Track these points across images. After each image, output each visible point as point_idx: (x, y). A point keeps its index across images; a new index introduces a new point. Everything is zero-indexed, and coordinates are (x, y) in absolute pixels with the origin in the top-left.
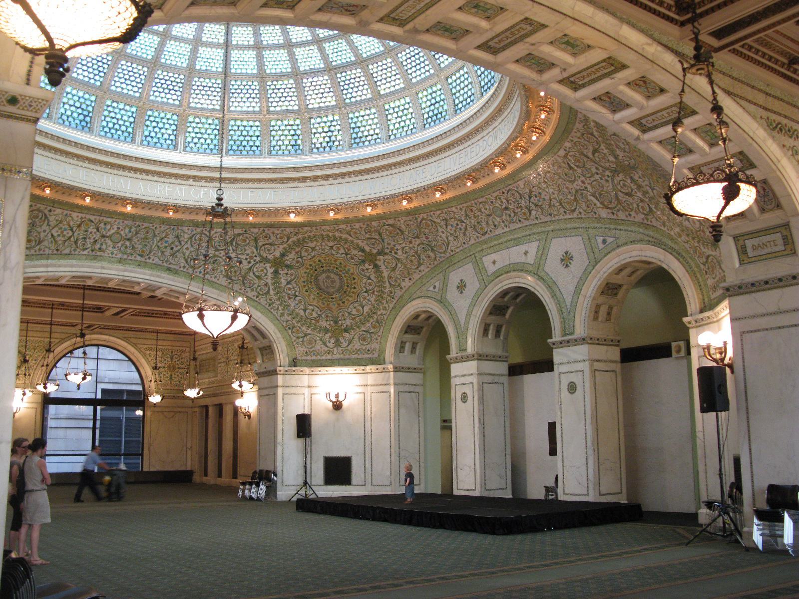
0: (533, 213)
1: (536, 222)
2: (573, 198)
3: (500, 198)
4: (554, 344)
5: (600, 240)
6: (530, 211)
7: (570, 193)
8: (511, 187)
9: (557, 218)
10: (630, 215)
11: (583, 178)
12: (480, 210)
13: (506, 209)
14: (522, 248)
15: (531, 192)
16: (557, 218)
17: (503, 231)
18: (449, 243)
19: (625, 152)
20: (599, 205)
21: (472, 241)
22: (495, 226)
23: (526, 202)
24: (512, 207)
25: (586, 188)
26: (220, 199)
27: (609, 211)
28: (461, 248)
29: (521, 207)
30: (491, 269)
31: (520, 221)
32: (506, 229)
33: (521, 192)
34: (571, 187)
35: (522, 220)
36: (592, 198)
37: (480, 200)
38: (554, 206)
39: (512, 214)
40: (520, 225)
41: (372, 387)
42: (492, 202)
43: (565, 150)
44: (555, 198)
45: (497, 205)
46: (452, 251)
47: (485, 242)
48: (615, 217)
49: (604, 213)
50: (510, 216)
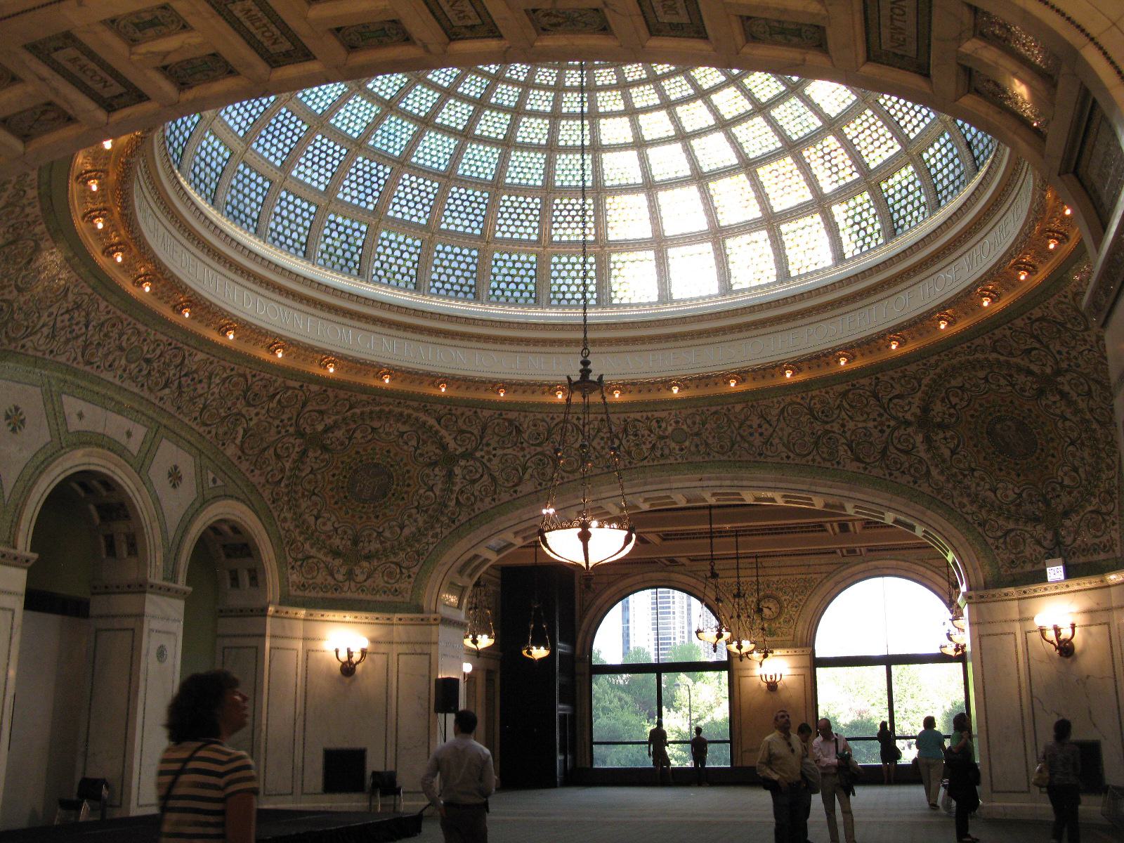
0: (167, 391)
1: (157, 402)
2: (223, 414)
3: (158, 345)
4: (152, 586)
5: (211, 476)
6: (166, 386)
7: (229, 409)
8: (185, 347)
9: (181, 416)
10: (252, 471)
11: (263, 412)
12: (121, 335)
13: (148, 361)
14: (127, 424)
15: (196, 371)
16: (181, 416)
17: (111, 379)
18: (36, 333)
19: (350, 439)
20: (238, 441)
21: (62, 359)
22: (110, 366)
23: (174, 375)
24: (155, 365)
25: (251, 419)
26: (585, 363)
27: (240, 453)
28: (39, 354)
29: (164, 374)
30: (75, 424)
31: (143, 385)
32: (117, 382)
33: (186, 361)
34: (238, 405)
35: (146, 387)
36: (241, 432)
37: (140, 326)
38: (194, 404)
39: (145, 372)
40: (136, 390)
41: (406, 657)
42: (145, 340)
43: (301, 386)
44: (206, 400)
45: (145, 349)
46: (23, 346)
47: (75, 373)
48: (236, 462)
49: (231, 451)
50: (140, 371)
